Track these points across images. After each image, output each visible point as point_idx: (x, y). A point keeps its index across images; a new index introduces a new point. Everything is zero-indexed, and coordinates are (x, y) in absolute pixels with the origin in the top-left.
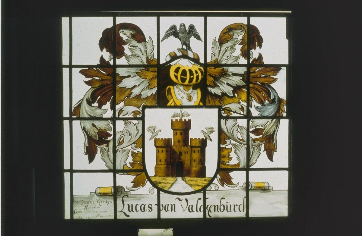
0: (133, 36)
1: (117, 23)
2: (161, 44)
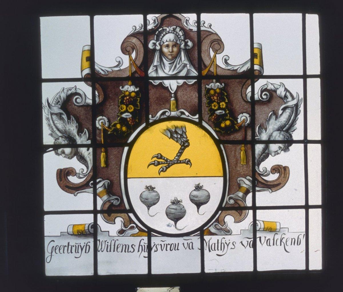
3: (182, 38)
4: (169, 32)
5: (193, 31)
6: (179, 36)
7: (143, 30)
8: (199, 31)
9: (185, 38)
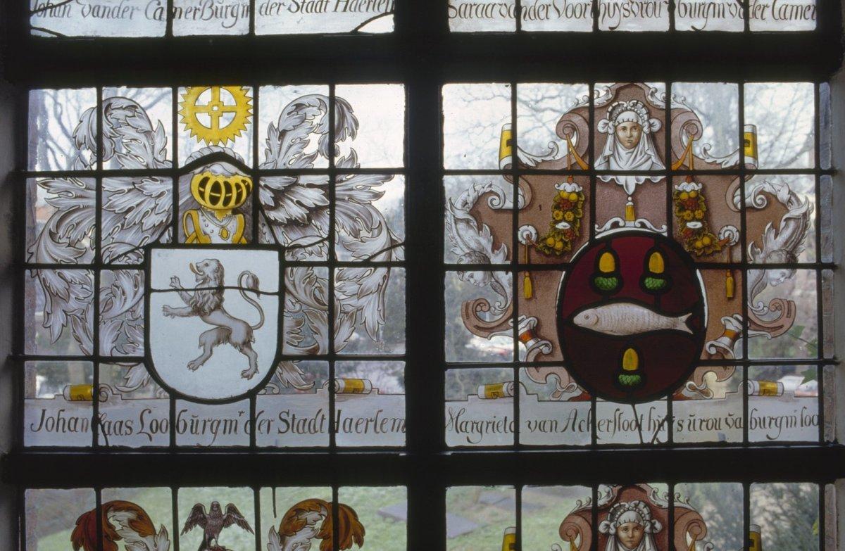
0: (132, 524)
1: (103, 502)
2: (181, 539)
3: (647, 517)
4: (629, 510)
5: (663, 507)
6: (643, 515)
7: (591, 506)
8: (671, 508)
9: (652, 518)
